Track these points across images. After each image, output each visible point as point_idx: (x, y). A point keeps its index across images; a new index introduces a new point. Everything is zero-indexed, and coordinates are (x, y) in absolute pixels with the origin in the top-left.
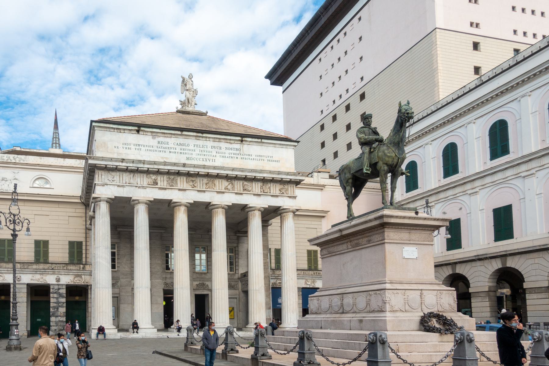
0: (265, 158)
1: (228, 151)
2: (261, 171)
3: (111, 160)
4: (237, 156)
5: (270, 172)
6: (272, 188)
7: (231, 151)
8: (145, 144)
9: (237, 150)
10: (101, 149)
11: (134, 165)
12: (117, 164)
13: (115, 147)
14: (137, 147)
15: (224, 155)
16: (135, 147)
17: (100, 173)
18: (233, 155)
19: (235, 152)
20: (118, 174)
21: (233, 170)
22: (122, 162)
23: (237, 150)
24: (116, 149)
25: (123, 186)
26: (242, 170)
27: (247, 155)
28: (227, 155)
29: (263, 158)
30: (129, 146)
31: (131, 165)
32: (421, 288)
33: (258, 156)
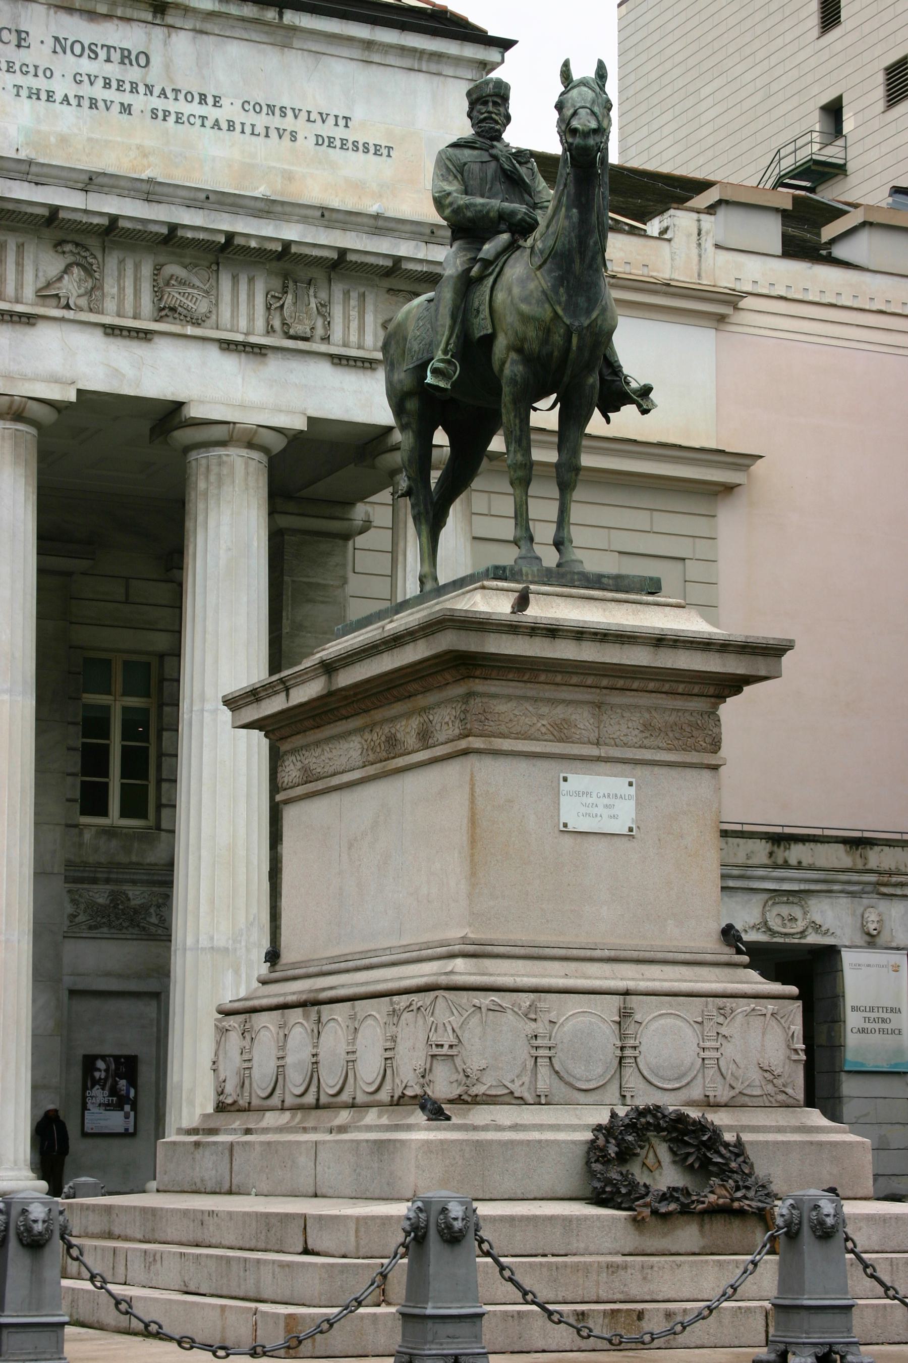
0: (300, 126)
1: (69, 63)
2: (268, 208)
4: (127, 98)
5: (326, 216)
6: (337, 312)
7: (86, 65)
9: (126, 57)
15: (41, 83)
18: (98, 91)
19: (113, 70)
21: (91, 182)
23: (126, 57)
26: (150, 191)
27: (189, 97)
28: (61, 87)
29: (289, 123)
32: (622, 985)
33: (257, 108)
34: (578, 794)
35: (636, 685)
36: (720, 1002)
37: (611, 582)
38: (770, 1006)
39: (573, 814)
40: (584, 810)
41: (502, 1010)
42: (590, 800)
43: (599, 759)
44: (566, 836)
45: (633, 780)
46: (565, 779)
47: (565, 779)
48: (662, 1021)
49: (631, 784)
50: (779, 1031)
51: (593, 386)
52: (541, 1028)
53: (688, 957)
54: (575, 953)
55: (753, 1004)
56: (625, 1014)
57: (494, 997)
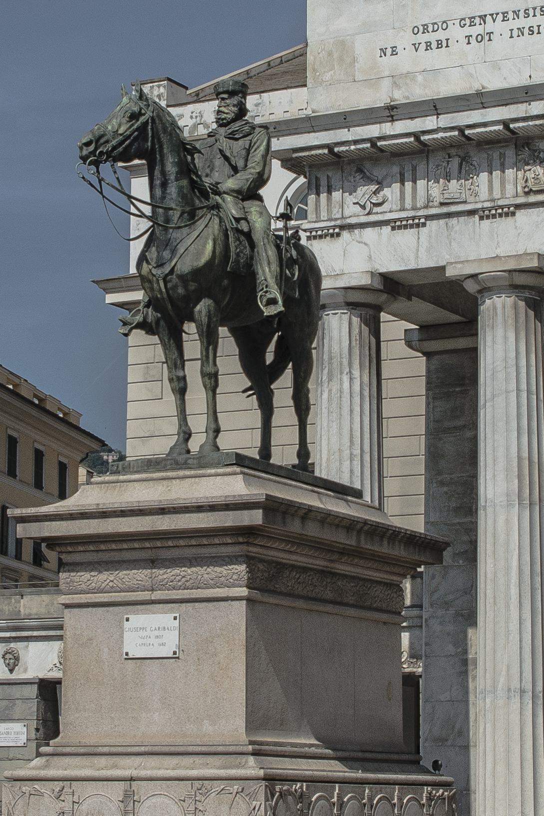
3: (345, 119)
8: (509, 7)
10: (327, 77)
11: (445, 120)
12: (372, 131)
13: (383, 51)
14: (478, 30)
16: (468, 30)
17: (324, 182)
20: (396, 169)
22: (392, 119)
24: (388, 60)
25: (414, 223)
30: (441, 35)
31: (430, 123)
32: (127, 773)
34: (136, 629)
35: (170, 543)
36: (197, 784)
37: (195, 461)
38: (236, 787)
39: (133, 645)
40: (141, 641)
41: (41, 795)
42: (145, 634)
43: (153, 602)
44: (130, 661)
45: (177, 615)
46: (128, 620)
47: (128, 620)
48: (154, 800)
49: (175, 618)
50: (243, 806)
51: (200, 312)
52: (67, 806)
53: (204, 749)
54: (130, 750)
55: (221, 785)
56: (128, 797)
57: (37, 786)
